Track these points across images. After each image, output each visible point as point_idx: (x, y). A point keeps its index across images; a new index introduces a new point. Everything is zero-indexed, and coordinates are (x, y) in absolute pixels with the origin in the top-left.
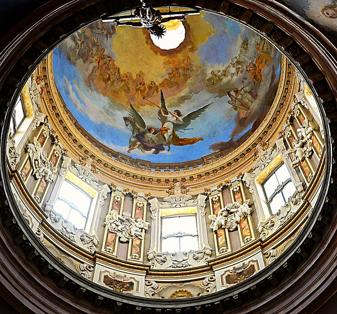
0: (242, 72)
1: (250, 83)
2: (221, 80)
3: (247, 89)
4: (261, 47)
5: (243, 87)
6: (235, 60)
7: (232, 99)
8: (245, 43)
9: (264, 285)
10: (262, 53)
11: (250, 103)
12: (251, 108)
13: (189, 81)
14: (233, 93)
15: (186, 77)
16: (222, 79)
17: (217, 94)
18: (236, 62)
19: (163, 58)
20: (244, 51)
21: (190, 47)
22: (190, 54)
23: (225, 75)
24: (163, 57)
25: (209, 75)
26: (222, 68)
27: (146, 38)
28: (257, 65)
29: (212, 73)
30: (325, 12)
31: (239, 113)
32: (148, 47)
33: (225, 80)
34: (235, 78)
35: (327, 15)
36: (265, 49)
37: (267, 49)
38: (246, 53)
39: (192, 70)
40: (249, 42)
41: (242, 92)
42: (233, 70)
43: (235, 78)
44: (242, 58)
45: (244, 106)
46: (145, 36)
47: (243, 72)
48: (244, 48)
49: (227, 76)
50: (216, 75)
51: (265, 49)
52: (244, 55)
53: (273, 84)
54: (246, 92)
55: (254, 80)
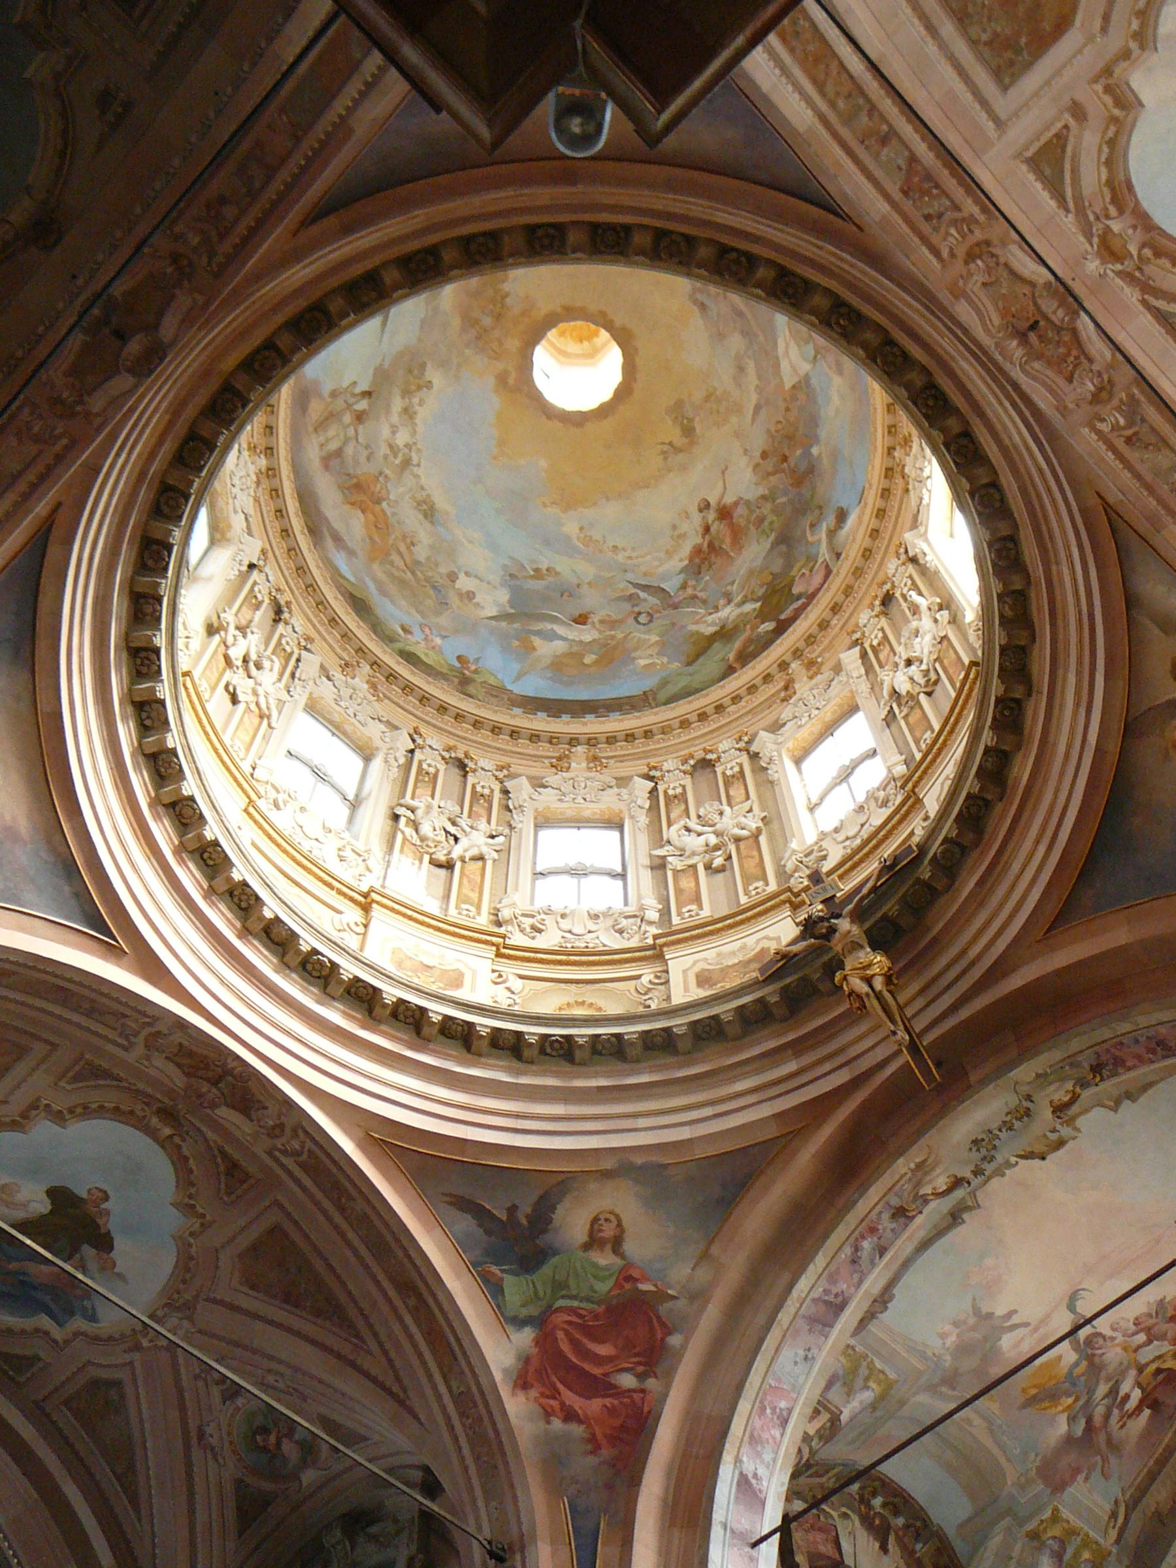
0: (386, 457)
1: (356, 462)
2: (406, 393)
3: (349, 450)
4: (403, 548)
5: (360, 440)
6: (415, 461)
7: (353, 395)
8: (429, 511)
9: (148, 609)
10: (391, 542)
11: (322, 439)
12: (314, 436)
13: (456, 322)
14: (363, 405)
15: (469, 321)
16: (403, 397)
17: (386, 366)
18: (410, 459)
19: (544, 307)
20: (420, 496)
21: (511, 381)
22: (500, 366)
23: (406, 410)
24: (544, 312)
25: (434, 375)
26: (423, 414)
27: (612, 321)
28: (377, 508)
29: (429, 385)
30: (612, 1217)
31: (320, 396)
32: (593, 308)
33: (397, 404)
34: (386, 432)
35: (608, 1216)
36: (395, 557)
37: (392, 563)
38: (413, 498)
39: (467, 346)
40: (427, 525)
41: (351, 432)
42: (402, 438)
43: (386, 432)
44: (408, 480)
45: (327, 419)
46: (618, 323)
47: (381, 459)
48: (425, 502)
49: (400, 415)
50: (419, 388)
51: (395, 557)
52: (411, 489)
53: (327, 534)
54: (347, 441)
55: (355, 481)
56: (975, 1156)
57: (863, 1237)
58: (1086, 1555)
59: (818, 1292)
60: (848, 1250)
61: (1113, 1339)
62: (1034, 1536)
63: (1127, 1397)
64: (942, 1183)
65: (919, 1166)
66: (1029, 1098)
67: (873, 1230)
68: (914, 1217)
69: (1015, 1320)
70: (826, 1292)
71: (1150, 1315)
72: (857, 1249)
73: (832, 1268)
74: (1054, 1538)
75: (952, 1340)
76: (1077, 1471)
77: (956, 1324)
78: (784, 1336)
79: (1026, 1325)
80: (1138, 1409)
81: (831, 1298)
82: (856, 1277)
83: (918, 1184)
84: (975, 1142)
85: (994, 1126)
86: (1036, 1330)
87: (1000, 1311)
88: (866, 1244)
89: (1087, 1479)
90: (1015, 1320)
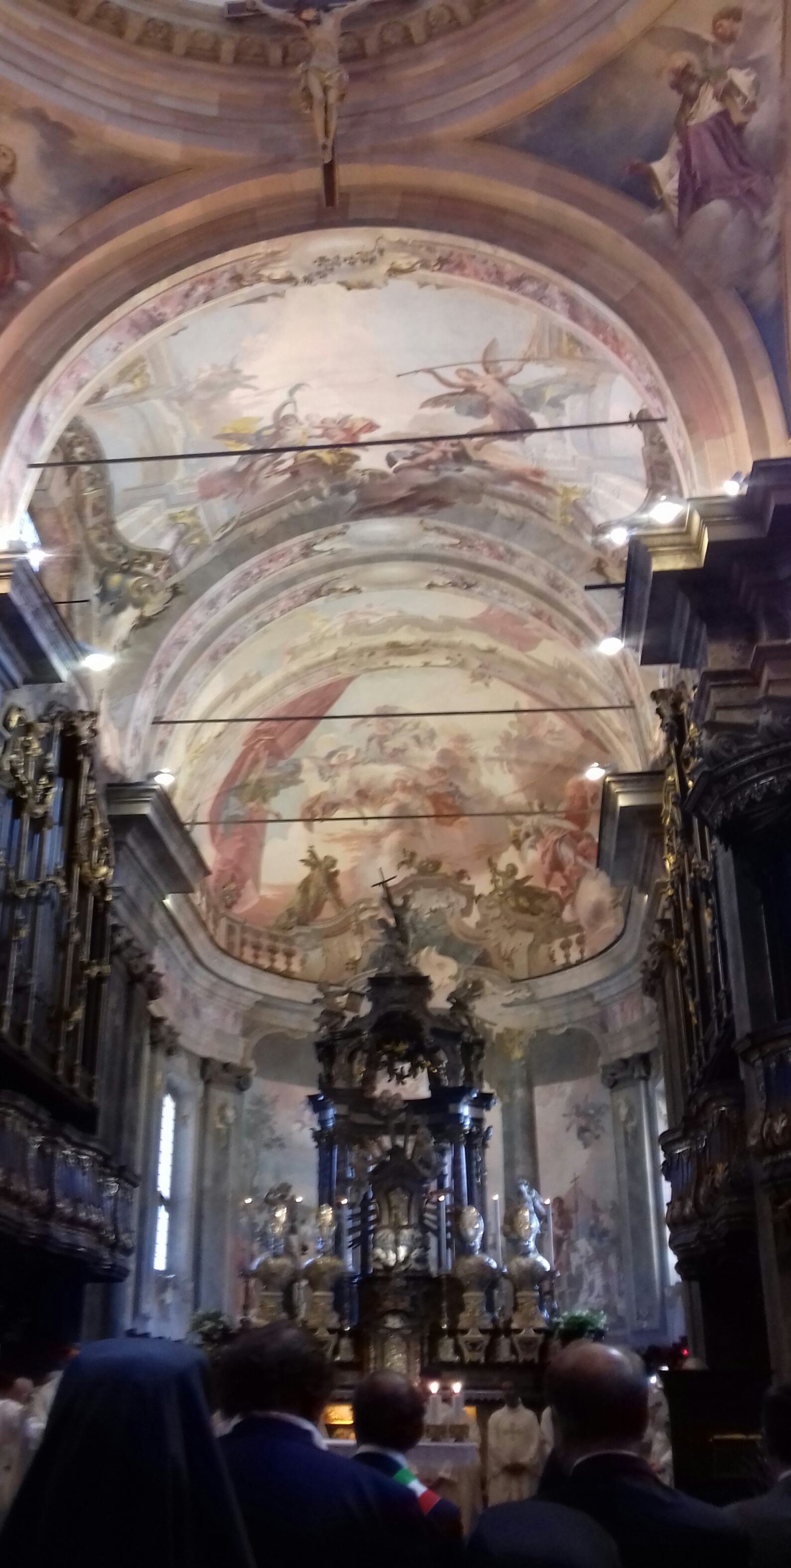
56: (315, 268)
57: (202, 282)
58: (197, 541)
59: (149, 306)
60: (186, 287)
61: (301, 424)
62: (173, 517)
63: (282, 462)
64: (279, 273)
65: (274, 254)
66: (381, 252)
67: (212, 281)
68: (245, 286)
69: (252, 382)
70: (155, 309)
71: (334, 421)
72: (193, 288)
73: (168, 294)
74: (185, 524)
75: (204, 376)
76: (223, 491)
77: (214, 366)
78: (111, 326)
79: (255, 388)
80: (284, 472)
81: (155, 314)
82: (180, 308)
83: (264, 266)
84: (322, 259)
85: (343, 256)
86: (259, 394)
87: (247, 372)
88: (201, 289)
89: (226, 498)
90: (252, 382)
